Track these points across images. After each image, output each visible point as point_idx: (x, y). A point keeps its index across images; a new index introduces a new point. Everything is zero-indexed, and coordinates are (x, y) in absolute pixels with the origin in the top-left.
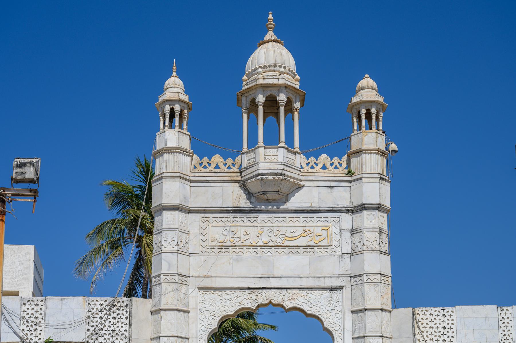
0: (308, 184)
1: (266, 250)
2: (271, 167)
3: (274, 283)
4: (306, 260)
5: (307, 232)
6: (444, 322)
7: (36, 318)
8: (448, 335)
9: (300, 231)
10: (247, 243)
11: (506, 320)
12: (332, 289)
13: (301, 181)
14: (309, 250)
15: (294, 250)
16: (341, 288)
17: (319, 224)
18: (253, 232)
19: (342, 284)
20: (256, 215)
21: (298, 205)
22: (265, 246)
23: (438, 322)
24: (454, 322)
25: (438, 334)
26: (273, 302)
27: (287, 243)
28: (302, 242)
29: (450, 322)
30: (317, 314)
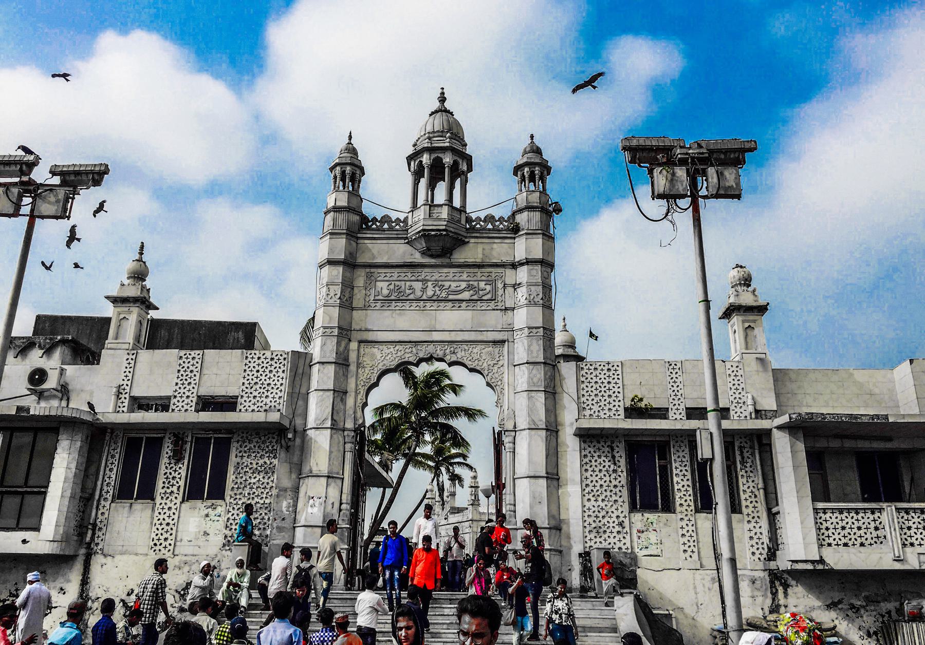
0: (472, 240)
1: (428, 304)
2: (435, 223)
3: (436, 336)
4: (469, 314)
5: (469, 288)
6: (609, 376)
7: (192, 371)
8: (614, 390)
9: (464, 285)
10: (411, 297)
11: (674, 376)
12: (495, 342)
13: (466, 237)
14: (471, 304)
15: (457, 305)
16: (504, 341)
17: (483, 278)
18: (418, 286)
19: (505, 338)
20: (420, 270)
21: (463, 260)
22: (430, 299)
23: (602, 376)
24: (620, 377)
25: (603, 389)
26: (435, 356)
27: (451, 297)
28: (466, 295)
29: (616, 377)
30: (478, 368)
